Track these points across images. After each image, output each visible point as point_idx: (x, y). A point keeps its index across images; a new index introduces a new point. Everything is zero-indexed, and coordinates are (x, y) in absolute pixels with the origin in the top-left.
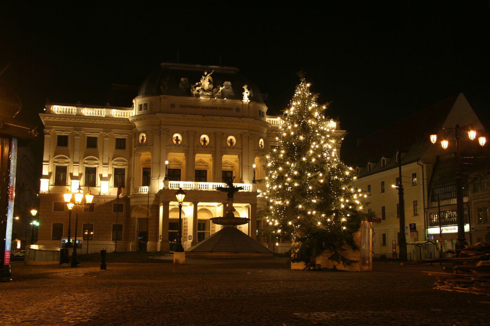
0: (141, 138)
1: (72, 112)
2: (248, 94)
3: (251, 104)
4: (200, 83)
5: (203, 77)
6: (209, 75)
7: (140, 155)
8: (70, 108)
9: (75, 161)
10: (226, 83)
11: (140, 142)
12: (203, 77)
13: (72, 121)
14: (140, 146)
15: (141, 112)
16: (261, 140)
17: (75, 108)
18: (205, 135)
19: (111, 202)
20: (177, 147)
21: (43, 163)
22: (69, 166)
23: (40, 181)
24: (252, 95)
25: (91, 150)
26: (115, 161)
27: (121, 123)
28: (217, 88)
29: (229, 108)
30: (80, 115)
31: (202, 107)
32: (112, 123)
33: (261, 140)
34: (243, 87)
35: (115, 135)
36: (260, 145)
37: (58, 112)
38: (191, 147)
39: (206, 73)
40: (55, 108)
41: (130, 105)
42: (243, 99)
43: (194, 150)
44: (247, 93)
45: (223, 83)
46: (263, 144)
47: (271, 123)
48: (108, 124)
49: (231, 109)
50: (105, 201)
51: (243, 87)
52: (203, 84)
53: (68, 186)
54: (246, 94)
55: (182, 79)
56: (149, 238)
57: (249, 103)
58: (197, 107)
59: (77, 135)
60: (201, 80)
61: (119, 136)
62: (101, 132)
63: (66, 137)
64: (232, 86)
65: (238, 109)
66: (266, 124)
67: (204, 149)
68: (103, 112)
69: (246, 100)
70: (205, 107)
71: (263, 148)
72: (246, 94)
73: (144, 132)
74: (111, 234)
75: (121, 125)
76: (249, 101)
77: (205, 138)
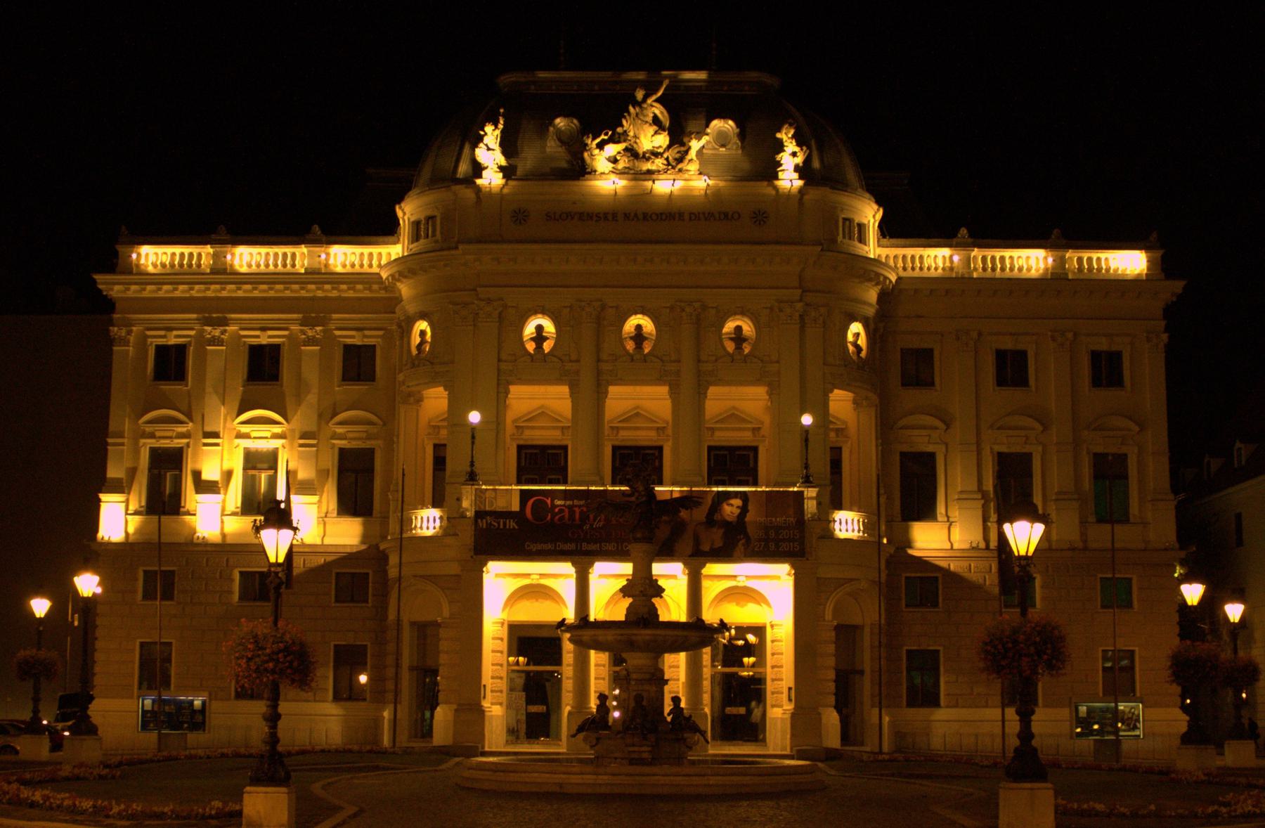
0: (416, 339)
1: (199, 265)
2: (799, 160)
3: (814, 194)
4: (619, 130)
5: (631, 108)
6: (654, 97)
7: (419, 400)
8: (195, 250)
9: (208, 429)
10: (716, 124)
11: (414, 352)
12: (631, 108)
13: (197, 291)
14: (413, 366)
15: (415, 247)
16: (856, 327)
17: (209, 249)
18: (639, 316)
19: (327, 566)
20: (540, 366)
21: (110, 440)
22: (188, 445)
23: (99, 501)
24: (816, 164)
25: (261, 388)
26: (340, 423)
27: (361, 292)
28: (683, 144)
29: (726, 215)
30: (223, 271)
32: (329, 291)
33: (856, 327)
34: (778, 135)
35: (337, 333)
36: (851, 348)
37: (155, 265)
38: (589, 360)
39: (640, 95)
40: (147, 255)
41: (385, 228)
42: (777, 178)
43: (599, 373)
44: (794, 154)
45: (707, 126)
46: (862, 342)
47: (891, 263)
48: (314, 300)
49: (736, 216)
50: (308, 565)
51: (778, 135)
52: (631, 134)
53: (189, 513)
54: (790, 158)
55: (558, 121)
57: (801, 191)
58: (610, 217)
59: (215, 341)
60: (624, 122)
61: (353, 337)
62: (295, 328)
63: (181, 350)
64: (742, 135)
65: (760, 217)
66: (868, 270)
67: (641, 363)
68: (300, 257)
69: (789, 179)
70: (636, 215)
71: (863, 354)
72: (790, 158)
73: (423, 316)
74: (327, 677)
75: (360, 299)
76: (800, 183)
77: (639, 327)
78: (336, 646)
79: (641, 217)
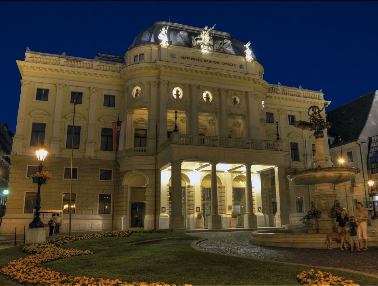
0: (134, 92)
11: (134, 96)
31: (205, 61)
49: (235, 65)
56: (147, 211)
58: (200, 60)
65: (241, 67)
70: (207, 61)
74: (97, 206)
78: (100, 195)
79: (209, 62)
